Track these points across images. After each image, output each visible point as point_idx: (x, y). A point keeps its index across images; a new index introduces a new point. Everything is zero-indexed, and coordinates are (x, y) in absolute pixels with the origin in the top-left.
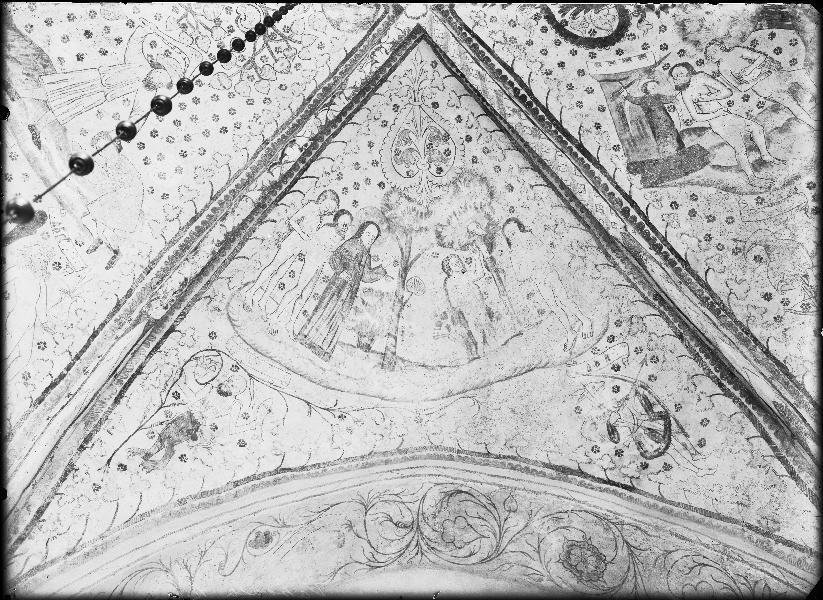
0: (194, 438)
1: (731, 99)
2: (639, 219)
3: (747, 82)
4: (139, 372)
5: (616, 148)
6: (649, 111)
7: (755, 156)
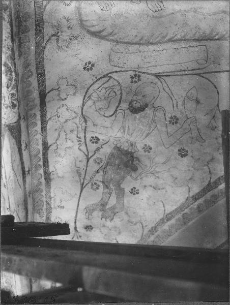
0: (135, 169)
4: (46, 147)
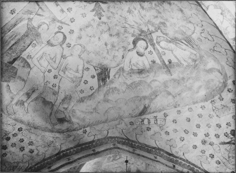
1: (53, 70)
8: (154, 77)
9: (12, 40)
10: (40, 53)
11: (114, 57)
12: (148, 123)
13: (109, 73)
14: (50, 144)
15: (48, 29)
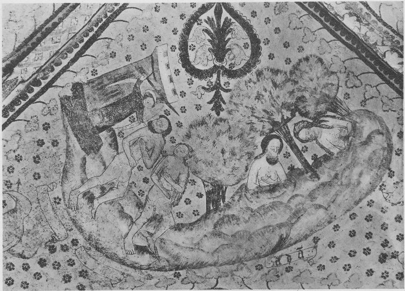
2: (30, 96)
3: (159, 180)
5: (94, 72)
6: (128, 99)
7: (97, 193)
8: (293, 191)
9: (113, 96)
10: (137, 135)
11: (234, 169)
12: (288, 261)
13: (224, 192)
14: (115, 282)
15: (154, 106)
